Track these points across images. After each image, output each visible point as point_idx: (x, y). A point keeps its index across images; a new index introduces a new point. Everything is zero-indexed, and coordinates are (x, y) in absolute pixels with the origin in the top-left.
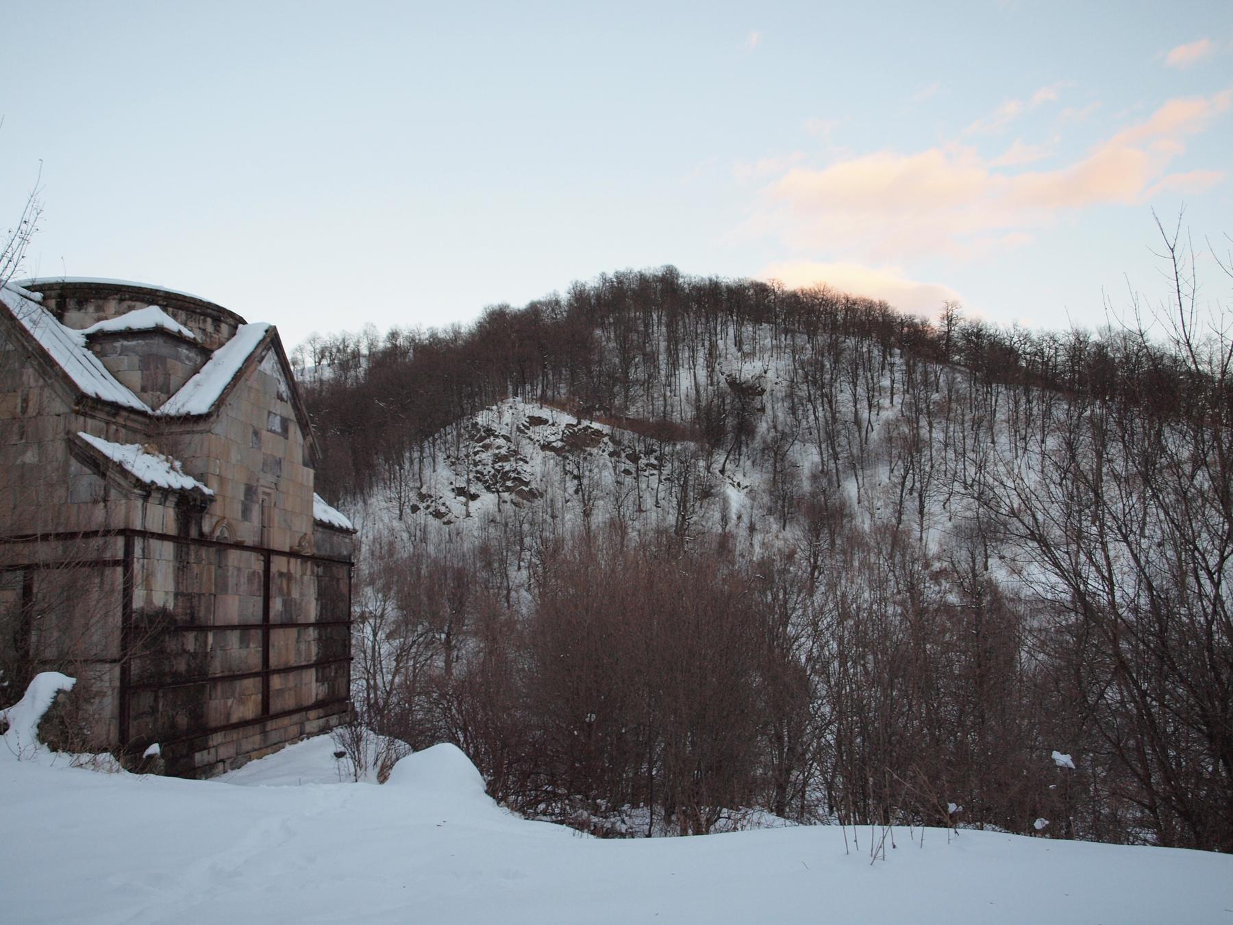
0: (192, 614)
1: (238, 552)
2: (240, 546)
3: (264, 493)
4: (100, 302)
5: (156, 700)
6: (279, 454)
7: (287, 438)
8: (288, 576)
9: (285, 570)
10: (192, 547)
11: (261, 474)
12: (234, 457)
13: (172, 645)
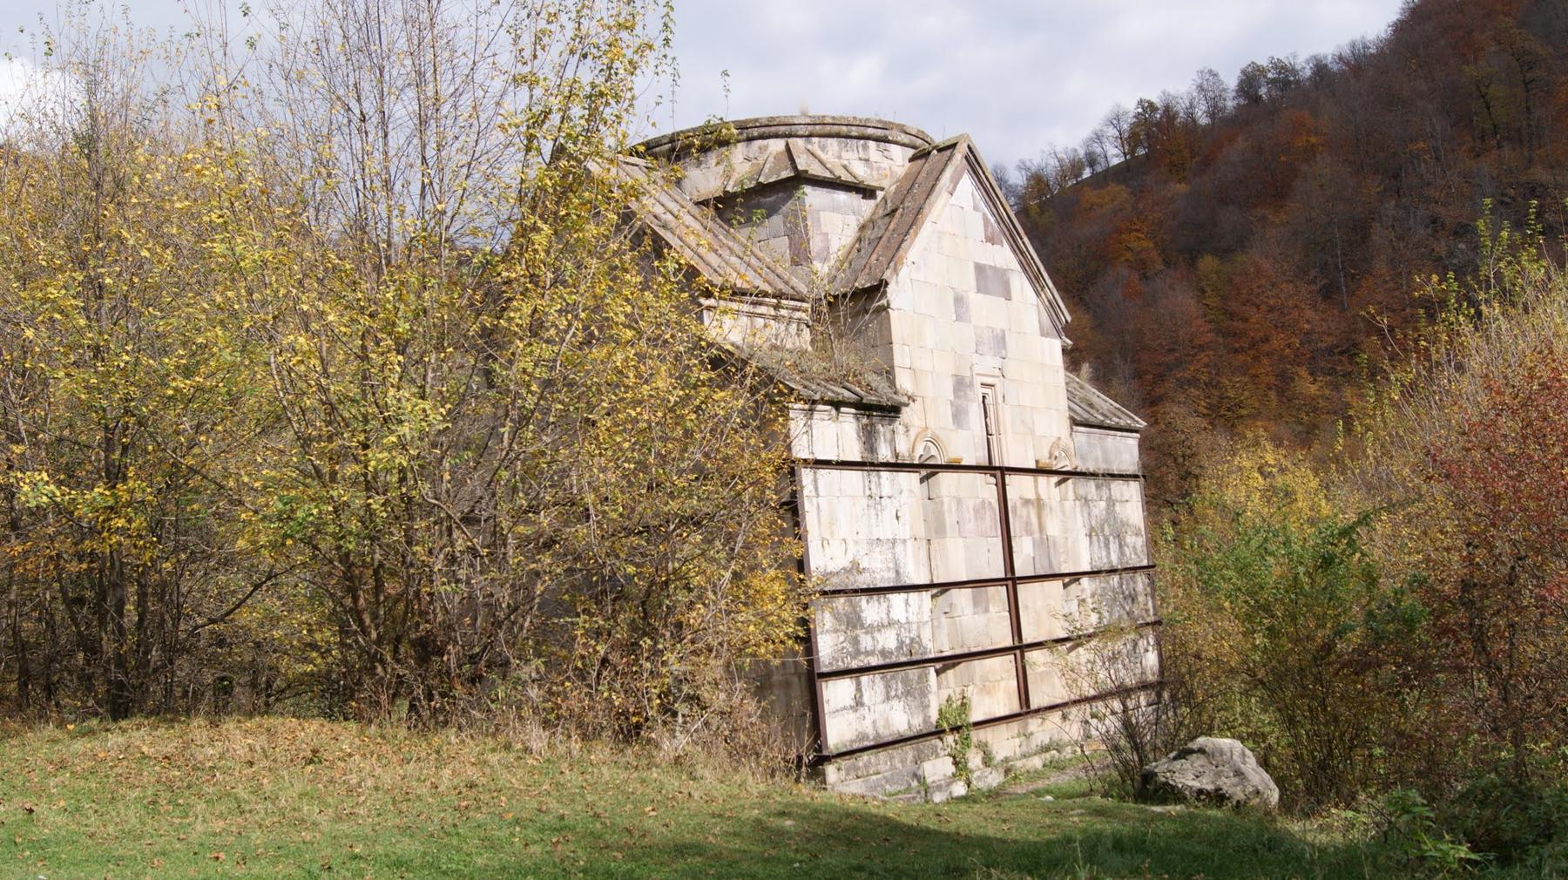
0: (897, 572)
5: (859, 689)
6: (999, 324)
7: (1008, 298)
8: (1039, 504)
9: (1031, 496)
11: (976, 358)
13: (871, 610)
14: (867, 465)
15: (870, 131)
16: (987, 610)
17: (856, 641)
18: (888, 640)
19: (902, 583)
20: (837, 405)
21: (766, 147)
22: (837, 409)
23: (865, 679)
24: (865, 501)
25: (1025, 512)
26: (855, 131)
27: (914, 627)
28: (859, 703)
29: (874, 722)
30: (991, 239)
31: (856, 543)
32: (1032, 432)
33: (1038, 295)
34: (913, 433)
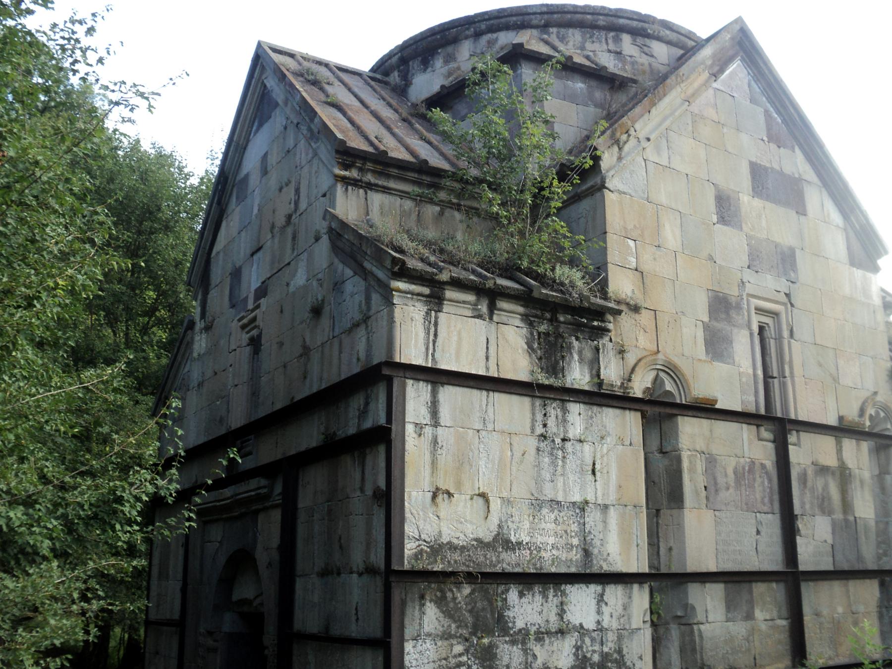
0: (587, 553)
1: (705, 423)
2: (705, 409)
3: (760, 310)
4: (450, 49)
8: (844, 475)
9: (830, 461)
10: (575, 409)
11: (748, 275)
12: (671, 236)
14: (546, 392)
15: (622, 21)
16: (749, 616)
19: (595, 570)
20: (492, 296)
21: (497, 39)
22: (492, 308)
24: (533, 442)
25: (820, 483)
26: (602, 21)
27: (611, 637)
30: (773, 138)
31: (507, 502)
32: (836, 380)
34: (631, 358)
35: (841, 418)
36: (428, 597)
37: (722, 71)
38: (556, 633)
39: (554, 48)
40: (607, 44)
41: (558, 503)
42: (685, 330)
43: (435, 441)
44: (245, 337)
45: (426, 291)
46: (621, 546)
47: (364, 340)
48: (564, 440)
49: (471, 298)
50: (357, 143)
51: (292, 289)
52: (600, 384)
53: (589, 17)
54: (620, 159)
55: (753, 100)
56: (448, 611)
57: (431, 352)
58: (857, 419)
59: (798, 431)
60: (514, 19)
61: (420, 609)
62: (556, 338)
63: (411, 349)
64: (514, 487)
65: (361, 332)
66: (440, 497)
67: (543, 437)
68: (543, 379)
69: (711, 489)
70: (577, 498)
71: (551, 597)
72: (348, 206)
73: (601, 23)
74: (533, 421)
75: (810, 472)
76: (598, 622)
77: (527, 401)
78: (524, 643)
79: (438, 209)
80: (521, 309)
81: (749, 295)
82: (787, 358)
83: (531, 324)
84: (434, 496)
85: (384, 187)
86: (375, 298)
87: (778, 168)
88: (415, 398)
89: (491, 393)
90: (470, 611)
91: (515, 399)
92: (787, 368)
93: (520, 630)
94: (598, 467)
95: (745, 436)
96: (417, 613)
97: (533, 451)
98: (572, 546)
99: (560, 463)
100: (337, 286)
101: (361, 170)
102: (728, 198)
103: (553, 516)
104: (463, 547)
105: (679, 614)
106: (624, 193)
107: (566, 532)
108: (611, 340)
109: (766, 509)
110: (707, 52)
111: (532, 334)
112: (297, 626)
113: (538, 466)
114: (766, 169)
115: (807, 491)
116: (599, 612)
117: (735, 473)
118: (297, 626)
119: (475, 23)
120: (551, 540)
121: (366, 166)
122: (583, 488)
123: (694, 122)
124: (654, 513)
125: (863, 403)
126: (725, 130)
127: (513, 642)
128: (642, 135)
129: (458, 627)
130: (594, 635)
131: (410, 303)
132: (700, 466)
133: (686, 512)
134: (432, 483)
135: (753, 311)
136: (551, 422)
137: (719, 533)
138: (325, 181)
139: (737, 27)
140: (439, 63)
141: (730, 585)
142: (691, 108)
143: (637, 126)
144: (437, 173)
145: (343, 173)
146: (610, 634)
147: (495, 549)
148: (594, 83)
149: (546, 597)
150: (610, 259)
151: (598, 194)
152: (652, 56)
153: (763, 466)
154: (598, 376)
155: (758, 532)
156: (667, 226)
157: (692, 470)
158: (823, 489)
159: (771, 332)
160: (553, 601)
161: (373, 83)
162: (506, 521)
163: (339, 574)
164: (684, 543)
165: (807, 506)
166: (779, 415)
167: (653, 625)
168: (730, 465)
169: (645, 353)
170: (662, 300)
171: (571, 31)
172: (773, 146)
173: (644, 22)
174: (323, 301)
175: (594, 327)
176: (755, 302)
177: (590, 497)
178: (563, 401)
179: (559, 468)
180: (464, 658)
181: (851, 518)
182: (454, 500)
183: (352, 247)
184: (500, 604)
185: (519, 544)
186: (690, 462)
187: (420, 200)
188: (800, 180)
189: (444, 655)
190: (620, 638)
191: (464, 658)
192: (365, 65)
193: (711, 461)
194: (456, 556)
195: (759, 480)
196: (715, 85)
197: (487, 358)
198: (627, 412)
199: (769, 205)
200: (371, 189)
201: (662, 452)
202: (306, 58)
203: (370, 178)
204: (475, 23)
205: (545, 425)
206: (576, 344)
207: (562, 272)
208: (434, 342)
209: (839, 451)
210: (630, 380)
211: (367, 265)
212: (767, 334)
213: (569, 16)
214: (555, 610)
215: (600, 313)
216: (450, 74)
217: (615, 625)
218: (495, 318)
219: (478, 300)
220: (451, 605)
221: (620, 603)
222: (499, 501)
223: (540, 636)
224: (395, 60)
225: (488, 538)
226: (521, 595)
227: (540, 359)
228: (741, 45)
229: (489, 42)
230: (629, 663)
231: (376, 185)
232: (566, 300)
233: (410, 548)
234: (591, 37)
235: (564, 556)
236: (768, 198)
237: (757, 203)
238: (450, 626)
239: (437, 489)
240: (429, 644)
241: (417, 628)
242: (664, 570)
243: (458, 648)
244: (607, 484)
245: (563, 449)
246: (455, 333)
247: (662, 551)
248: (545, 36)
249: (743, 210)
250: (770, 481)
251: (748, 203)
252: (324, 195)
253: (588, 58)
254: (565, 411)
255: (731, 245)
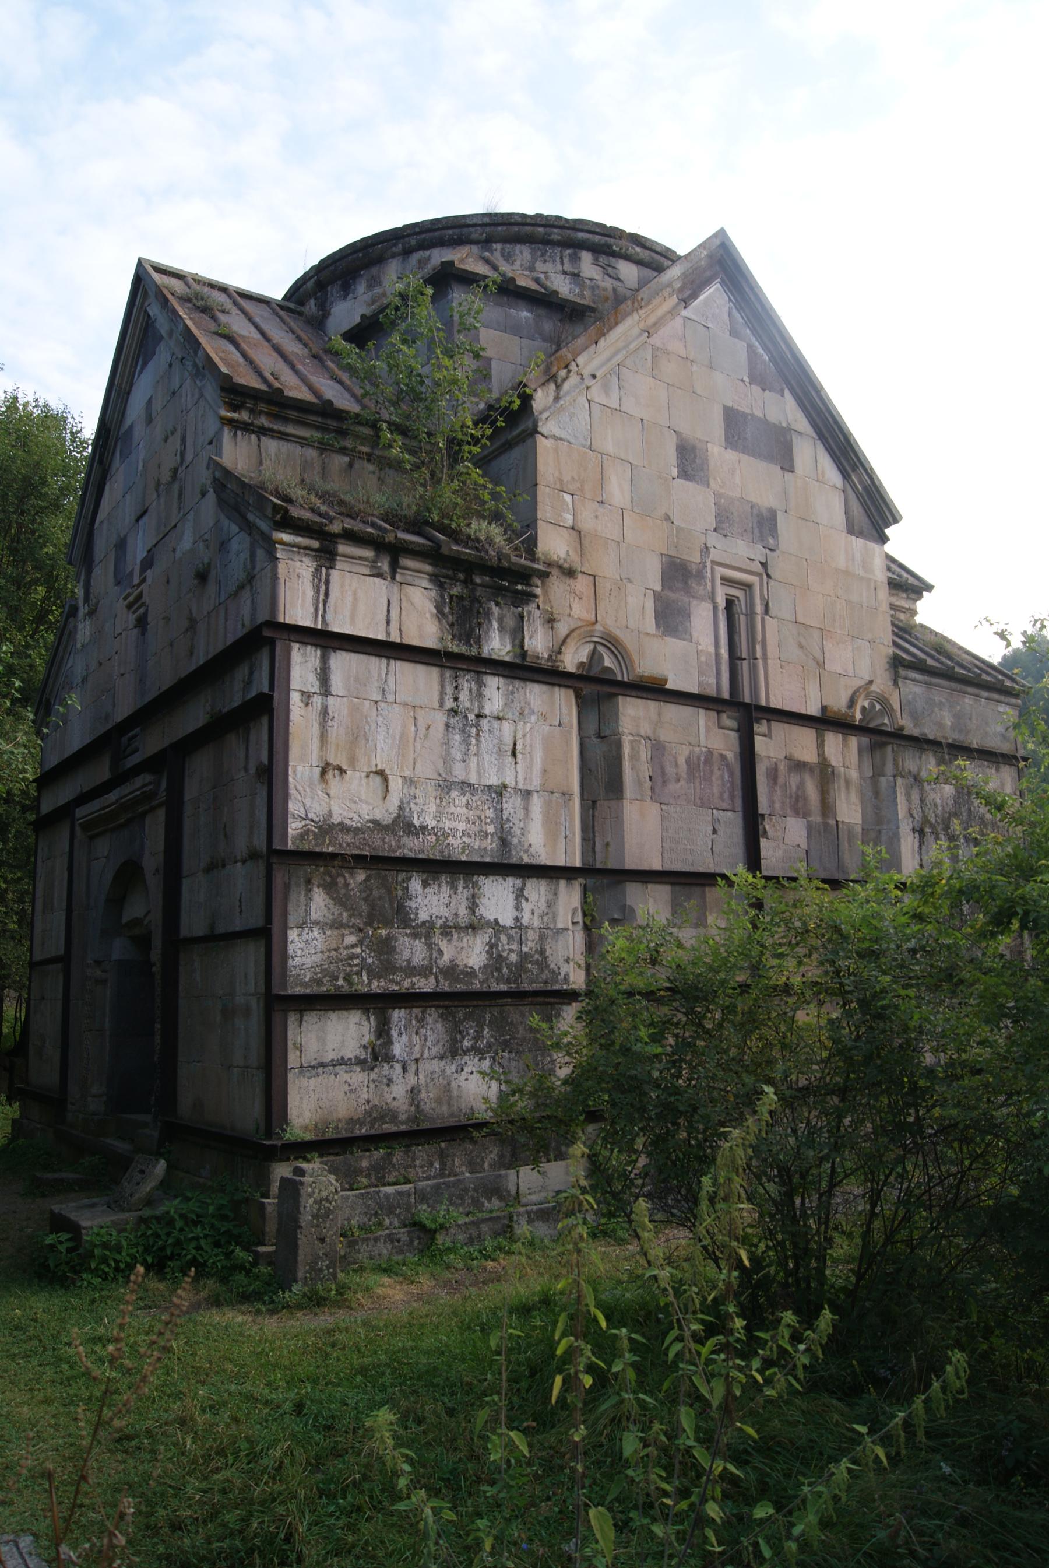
0: (504, 843)
1: (652, 705)
3: (726, 581)
4: (374, 271)
5: (383, 1031)
7: (788, 466)
8: (825, 773)
9: (809, 755)
11: (713, 540)
12: (618, 491)
14: (460, 662)
17: (385, 948)
18: (472, 954)
19: (514, 860)
21: (429, 258)
22: (394, 566)
23: (398, 1016)
24: (441, 718)
25: (794, 781)
26: (556, 235)
27: (532, 935)
28: (378, 1055)
29: (414, 1091)
30: (757, 378)
31: (410, 782)
32: (821, 664)
33: (845, 476)
34: (562, 629)
35: (824, 708)
36: (315, 881)
37: (694, 296)
38: (467, 928)
39: (495, 268)
40: (562, 263)
41: (471, 785)
42: (630, 599)
43: (325, 712)
44: (132, 618)
45: (315, 544)
46: (544, 838)
47: (249, 602)
48: (478, 716)
49: (369, 553)
50: (247, 379)
51: (178, 554)
52: (524, 654)
53: (541, 229)
54: (557, 398)
55: (734, 333)
56: (340, 900)
57: (320, 613)
58: (844, 710)
59: (768, 721)
60: (450, 232)
61: (306, 895)
62: (472, 602)
63: (297, 607)
64: (418, 765)
65: (246, 594)
66: (331, 773)
67: (454, 712)
68: (454, 647)
69: (658, 780)
70: (493, 780)
71: (460, 889)
72: (237, 454)
73: (555, 237)
74: (442, 693)
75: (782, 767)
76: (517, 919)
77: (435, 671)
78: (428, 937)
79: (347, 459)
80: (428, 568)
81: (713, 562)
82: (759, 637)
83: (441, 586)
84: (324, 772)
85: (280, 432)
86: (260, 553)
87: (761, 415)
88: (302, 666)
89: (392, 662)
90: (365, 900)
91: (421, 670)
92: (758, 648)
93: (424, 923)
94: (519, 748)
95: (702, 722)
96: (302, 898)
97: (441, 728)
98: (487, 834)
99: (474, 741)
100: (223, 546)
101: (252, 411)
102: (694, 448)
103: (464, 800)
104: (357, 828)
105: (616, 916)
106: (561, 439)
107: (479, 817)
108: (538, 607)
109: (725, 805)
110: (674, 273)
111: (442, 596)
112: (184, 932)
113: (447, 743)
114: (744, 415)
115: (777, 788)
116: (518, 908)
117: (688, 762)
118: (184, 932)
119: (403, 237)
120: (462, 826)
121: (259, 407)
122: (500, 769)
123: (655, 357)
124: (590, 805)
125: (855, 693)
126: (695, 368)
127: (415, 936)
128: (586, 373)
129: (350, 916)
130: (512, 932)
131: (297, 558)
132: (644, 754)
133: (626, 803)
134: (321, 757)
135: (718, 581)
136: (464, 696)
137: (665, 829)
138: (212, 425)
139: (718, 242)
140: (361, 288)
141: (677, 888)
142: (651, 341)
143: (580, 360)
144: (340, 415)
145: (230, 415)
146: (530, 933)
147: (394, 833)
148: (542, 312)
149: (454, 889)
150: (540, 515)
151: (529, 441)
152: (619, 279)
153: (723, 757)
154: (522, 646)
155: (715, 831)
156: (614, 480)
157: (634, 757)
158: (798, 788)
159: (741, 607)
160: (464, 892)
161: (282, 313)
162: (409, 803)
163: (224, 866)
164: (623, 837)
165: (777, 805)
166: (747, 700)
167: (586, 928)
168: (683, 754)
169: (580, 624)
170: (606, 565)
171: (518, 247)
172: (756, 389)
173: (609, 236)
174: (209, 564)
175: (517, 592)
176: (720, 571)
177: (510, 781)
178: (478, 673)
179: (473, 749)
180: (358, 950)
181: (833, 822)
182: (347, 777)
183: (236, 497)
184: (400, 893)
185: (424, 828)
186: (632, 748)
187: (323, 448)
188: (789, 429)
189: (334, 946)
190: (542, 938)
191: (358, 950)
192: (277, 292)
193: (658, 748)
194: (348, 838)
195: (717, 773)
196: (685, 313)
197: (388, 622)
198: (557, 689)
199: (745, 458)
200: (265, 435)
201: (600, 736)
202: (199, 280)
203: (264, 421)
204: (403, 237)
205: (456, 699)
206: (496, 610)
207: (479, 528)
208: (325, 602)
209: (821, 745)
210: (560, 653)
211: (251, 517)
212: (736, 609)
213: (516, 229)
214: (465, 903)
215: (525, 576)
216: (373, 302)
217: (537, 923)
218: (398, 577)
219: (377, 556)
220: (343, 891)
221: (543, 899)
222: (400, 780)
223: (448, 930)
224: (310, 284)
225: (387, 820)
226: (425, 884)
227: (452, 625)
228: (721, 263)
229: (419, 262)
230: (552, 966)
231: (271, 430)
232: (482, 559)
233: (294, 827)
234: (543, 255)
235: (476, 845)
236: (745, 450)
237: (731, 455)
238: (341, 914)
239: (328, 764)
240: (316, 933)
241: (303, 914)
242: (599, 866)
243: (351, 939)
244: (529, 767)
245: (477, 726)
246: (350, 593)
247: (598, 847)
248: (487, 254)
249: (712, 464)
250: (731, 774)
251: (719, 456)
252: (211, 443)
253: (537, 281)
254: (481, 684)
255: (694, 505)
